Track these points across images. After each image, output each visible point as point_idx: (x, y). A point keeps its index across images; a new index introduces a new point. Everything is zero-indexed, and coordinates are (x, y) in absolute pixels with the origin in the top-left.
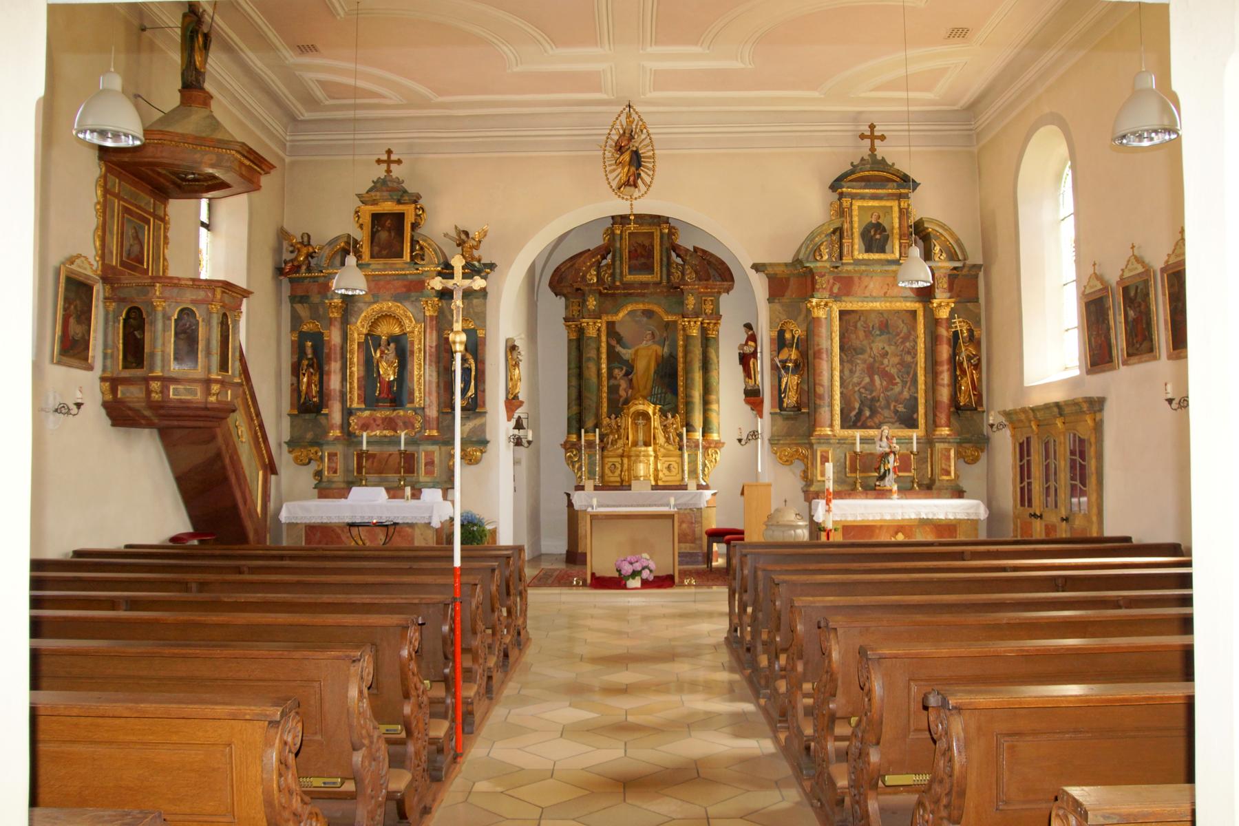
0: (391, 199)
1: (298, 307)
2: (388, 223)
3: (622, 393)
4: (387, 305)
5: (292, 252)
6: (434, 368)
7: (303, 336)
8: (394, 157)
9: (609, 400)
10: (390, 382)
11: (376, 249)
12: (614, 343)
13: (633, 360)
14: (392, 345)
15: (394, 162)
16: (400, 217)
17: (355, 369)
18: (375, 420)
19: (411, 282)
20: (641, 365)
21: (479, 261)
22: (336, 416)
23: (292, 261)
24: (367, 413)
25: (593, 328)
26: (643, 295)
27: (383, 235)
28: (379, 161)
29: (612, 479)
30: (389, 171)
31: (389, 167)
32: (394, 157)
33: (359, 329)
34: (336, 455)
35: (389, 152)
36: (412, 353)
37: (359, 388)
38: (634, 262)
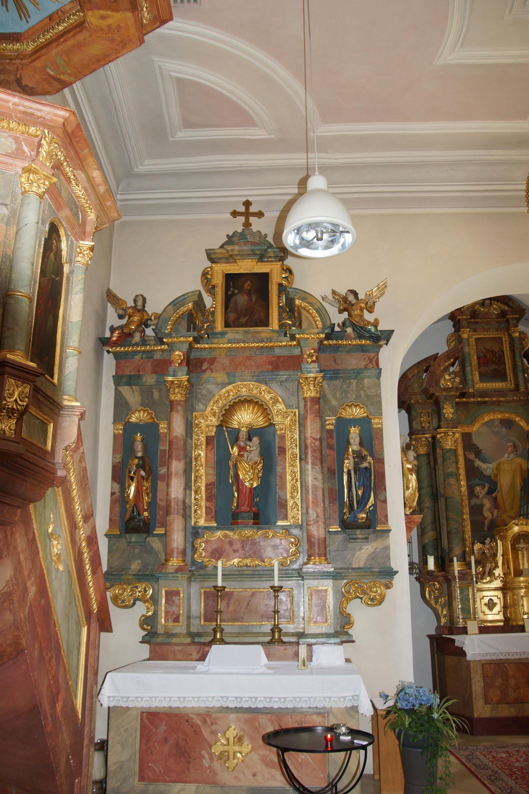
0: (253, 254)
1: (125, 390)
2: (247, 285)
3: (487, 514)
4: (246, 388)
5: (121, 317)
6: (318, 468)
7: (130, 430)
8: (252, 209)
9: (473, 523)
10: (251, 489)
11: (232, 316)
12: (472, 456)
13: (496, 476)
14: (256, 440)
15: (254, 214)
16: (264, 278)
17: (202, 471)
18: (231, 543)
19: (279, 357)
20: (504, 481)
21: (376, 326)
22: (177, 539)
23: (121, 327)
24: (219, 534)
25: (450, 440)
26: (498, 403)
27: (242, 299)
28: (235, 214)
29: (490, 618)
30: (247, 224)
31: (247, 219)
32: (252, 209)
33: (207, 421)
34: (178, 593)
35: (247, 204)
36: (283, 450)
37: (208, 499)
38: (484, 368)
